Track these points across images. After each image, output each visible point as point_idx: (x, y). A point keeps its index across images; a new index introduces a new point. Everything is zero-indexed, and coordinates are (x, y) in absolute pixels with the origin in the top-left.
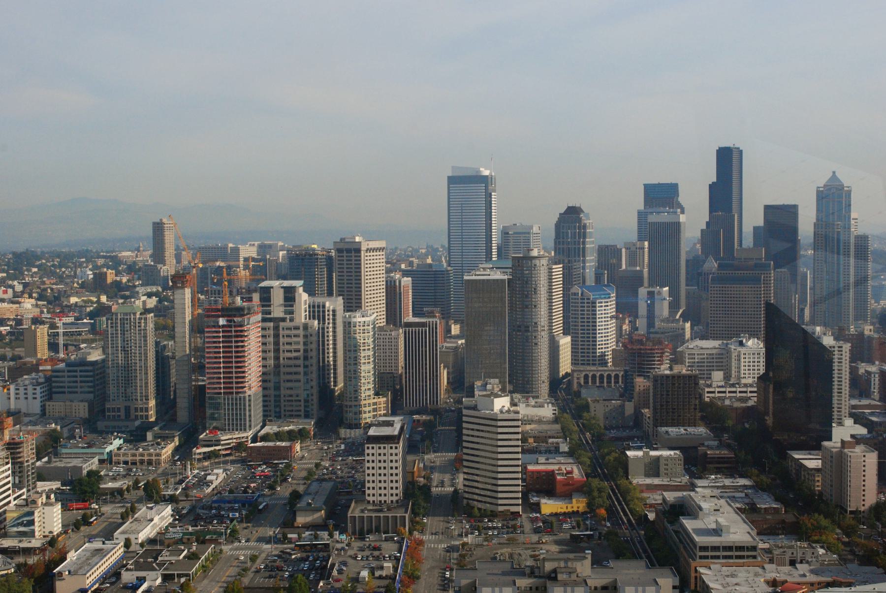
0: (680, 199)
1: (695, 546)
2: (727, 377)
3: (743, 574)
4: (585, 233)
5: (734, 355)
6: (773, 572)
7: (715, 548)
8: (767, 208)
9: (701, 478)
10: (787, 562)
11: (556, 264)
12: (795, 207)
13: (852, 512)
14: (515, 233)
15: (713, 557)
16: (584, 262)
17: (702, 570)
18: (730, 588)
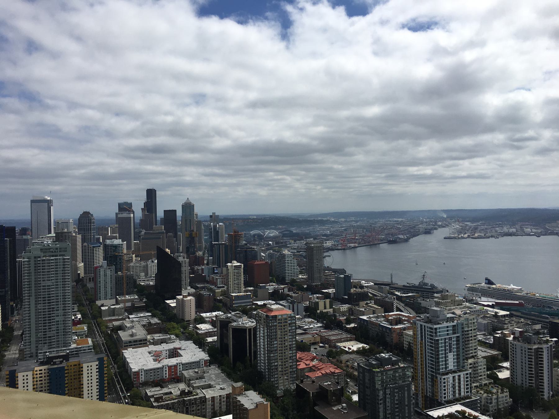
0: (132, 208)
1: (123, 342)
2: (146, 275)
3: (140, 350)
4: (91, 222)
5: (149, 265)
6: (152, 348)
7: (130, 342)
8: (165, 211)
9: (132, 314)
10: (159, 342)
11: (78, 234)
12: (175, 211)
13: (187, 321)
14: (62, 223)
15: (130, 346)
16: (91, 233)
17: (123, 351)
18: (134, 357)
